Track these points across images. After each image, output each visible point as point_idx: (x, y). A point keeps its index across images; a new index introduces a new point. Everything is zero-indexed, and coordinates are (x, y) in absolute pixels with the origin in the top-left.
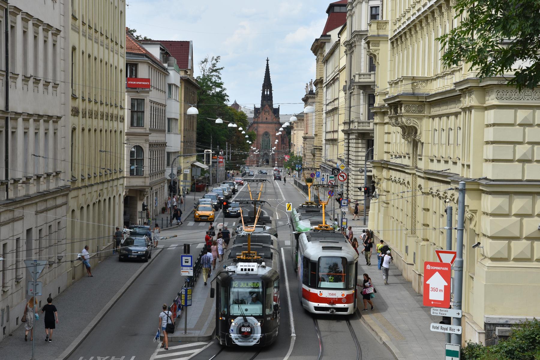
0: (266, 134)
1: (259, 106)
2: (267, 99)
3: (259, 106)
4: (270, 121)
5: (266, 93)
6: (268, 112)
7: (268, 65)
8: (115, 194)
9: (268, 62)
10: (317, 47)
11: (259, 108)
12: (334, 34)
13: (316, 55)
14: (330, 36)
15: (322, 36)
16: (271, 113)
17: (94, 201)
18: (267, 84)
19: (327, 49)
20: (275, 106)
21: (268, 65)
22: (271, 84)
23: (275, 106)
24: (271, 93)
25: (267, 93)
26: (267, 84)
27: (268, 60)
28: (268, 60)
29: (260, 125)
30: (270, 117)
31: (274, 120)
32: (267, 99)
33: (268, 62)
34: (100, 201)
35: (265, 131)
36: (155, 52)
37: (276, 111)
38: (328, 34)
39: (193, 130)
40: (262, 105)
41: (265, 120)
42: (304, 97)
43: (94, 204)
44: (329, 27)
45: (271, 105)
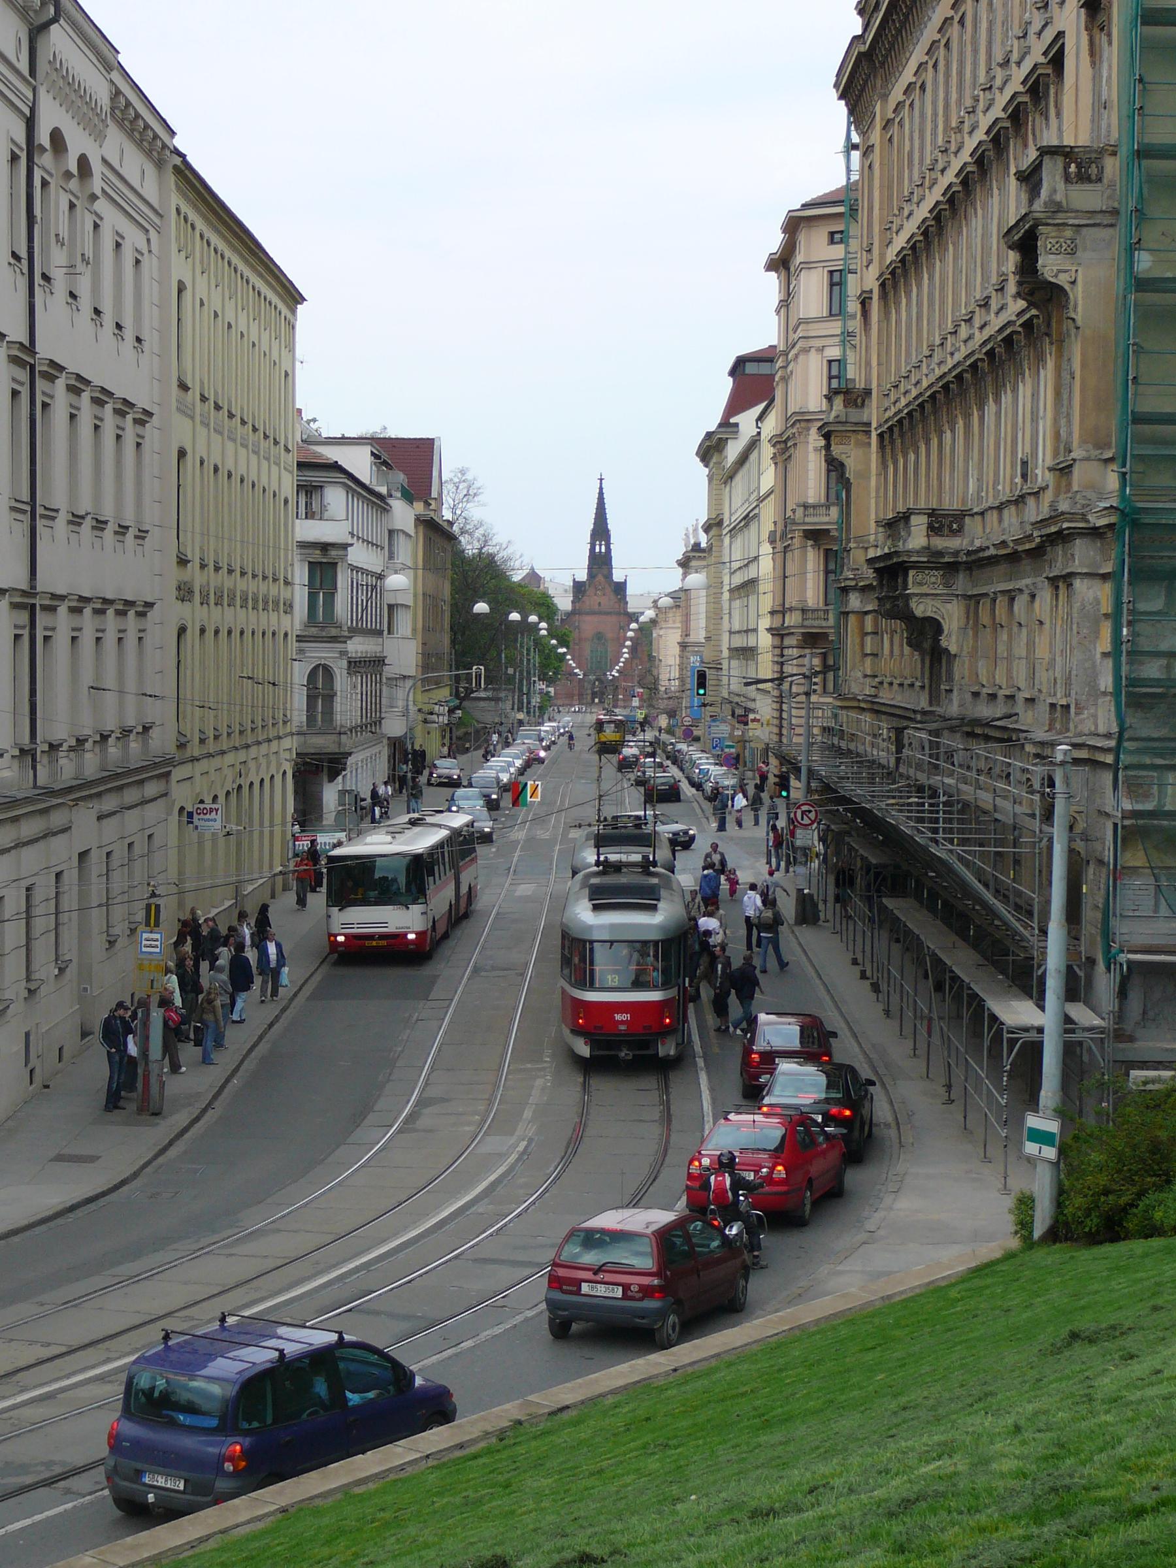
0: (599, 636)
1: (582, 576)
2: (600, 562)
3: (582, 576)
5: (597, 550)
7: (601, 489)
8: (273, 771)
10: (710, 449)
12: (746, 421)
13: (706, 466)
14: (736, 425)
15: (720, 425)
16: (609, 590)
17: (229, 786)
18: (601, 531)
19: (733, 450)
20: (617, 576)
21: (601, 489)
22: (608, 531)
23: (617, 576)
24: (608, 549)
25: (600, 548)
26: (601, 531)
27: (601, 480)
28: (601, 480)
29: (588, 618)
30: (607, 601)
32: (600, 562)
34: (240, 787)
36: (360, 463)
37: (620, 588)
38: (732, 420)
39: (442, 629)
40: (591, 575)
42: (680, 557)
43: (228, 793)
44: (736, 404)
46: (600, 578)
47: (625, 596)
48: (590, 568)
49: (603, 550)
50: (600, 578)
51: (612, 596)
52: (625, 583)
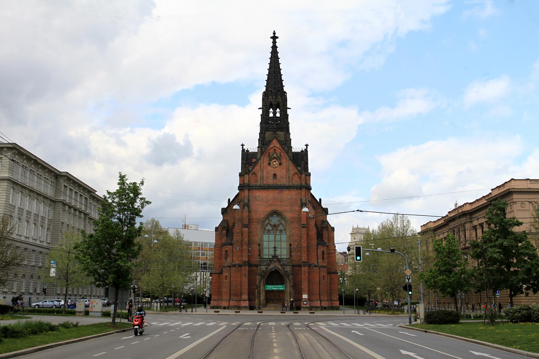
1: (253, 146)
3: (253, 146)
4: (284, 182)
5: (271, 115)
6: (279, 158)
7: (274, 47)
9: (274, 42)
11: (254, 153)
20: (297, 146)
21: (274, 47)
23: (297, 146)
24: (285, 116)
25: (274, 113)
27: (274, 38)
28: (274, 38)
30: (283, 172)
31: (296, 178)
33: (274, 42)
35: (269, 209)
37: (301, 160)
41: (271, 181)
45: (286, 142)
46: (275, 143)
47: (307, 168)
48: (262, 134)
49: (278, 115)
50: (275, 143)
51: (292, 167)
52: (306, 150)
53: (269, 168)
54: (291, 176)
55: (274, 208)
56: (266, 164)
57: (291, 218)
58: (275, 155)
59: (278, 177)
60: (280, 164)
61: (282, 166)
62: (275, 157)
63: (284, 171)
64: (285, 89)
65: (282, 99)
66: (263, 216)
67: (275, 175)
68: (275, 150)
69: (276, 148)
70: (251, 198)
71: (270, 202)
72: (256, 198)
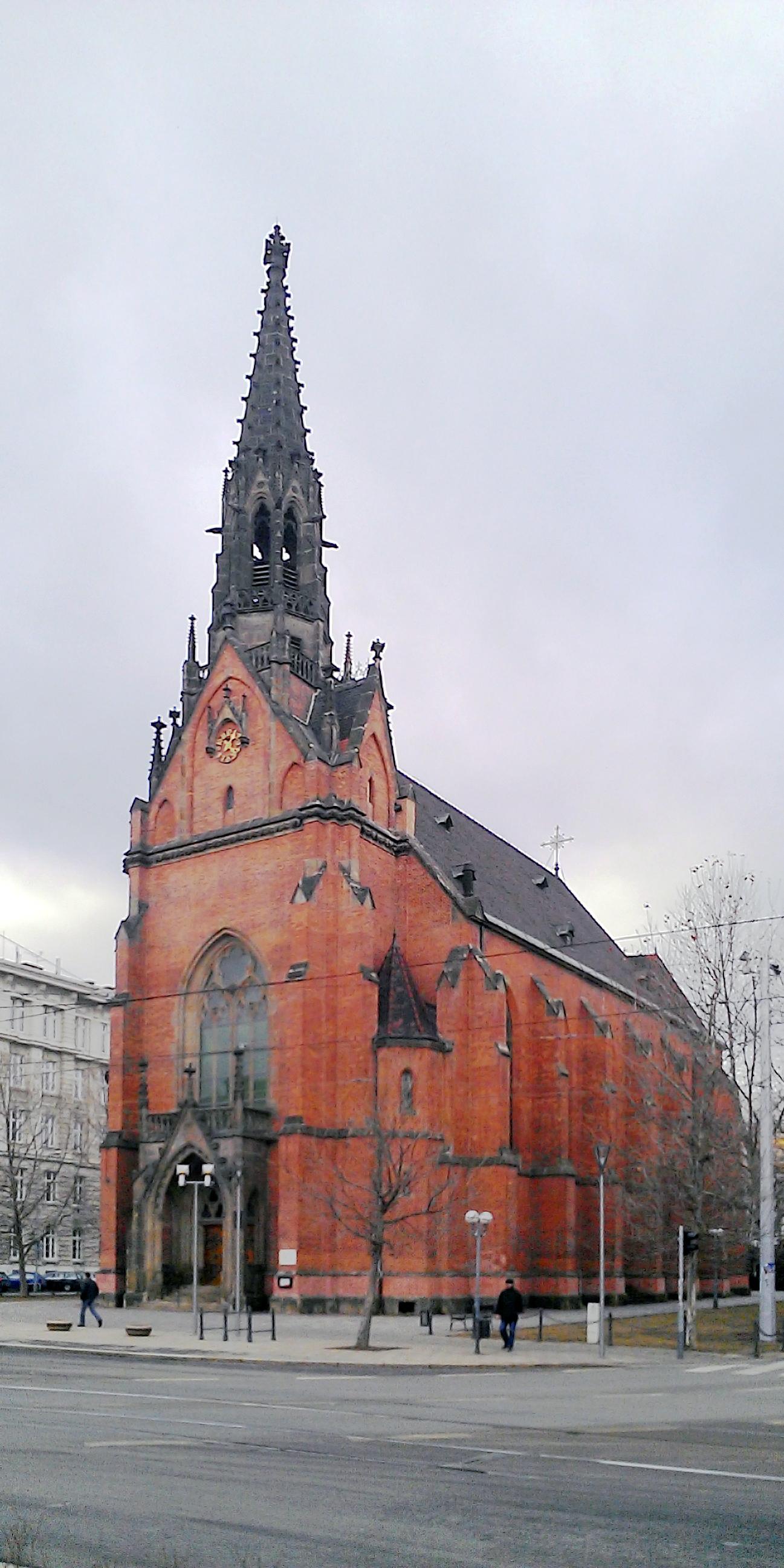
7: (276, 297)
21: (276, 297)
35: (207, 930)
53: (213, 768)
54: (276, 781)
55: (221, 922)
56: (201, 754)
57: (278, 949)
58: (227, 714)
59: (238, 799)
60: (244, 742)
61: (251, 750)
62: (228, 721)
63: (258, 767)
64: (312, 443)
65: (273, 485)
66: (188, 957)
67: (230, 788)
68: (226, 689)
69: (231, 685)
70: (152, 901)
71: (209, 902)
72: (167, 897)
